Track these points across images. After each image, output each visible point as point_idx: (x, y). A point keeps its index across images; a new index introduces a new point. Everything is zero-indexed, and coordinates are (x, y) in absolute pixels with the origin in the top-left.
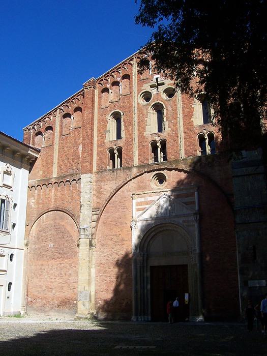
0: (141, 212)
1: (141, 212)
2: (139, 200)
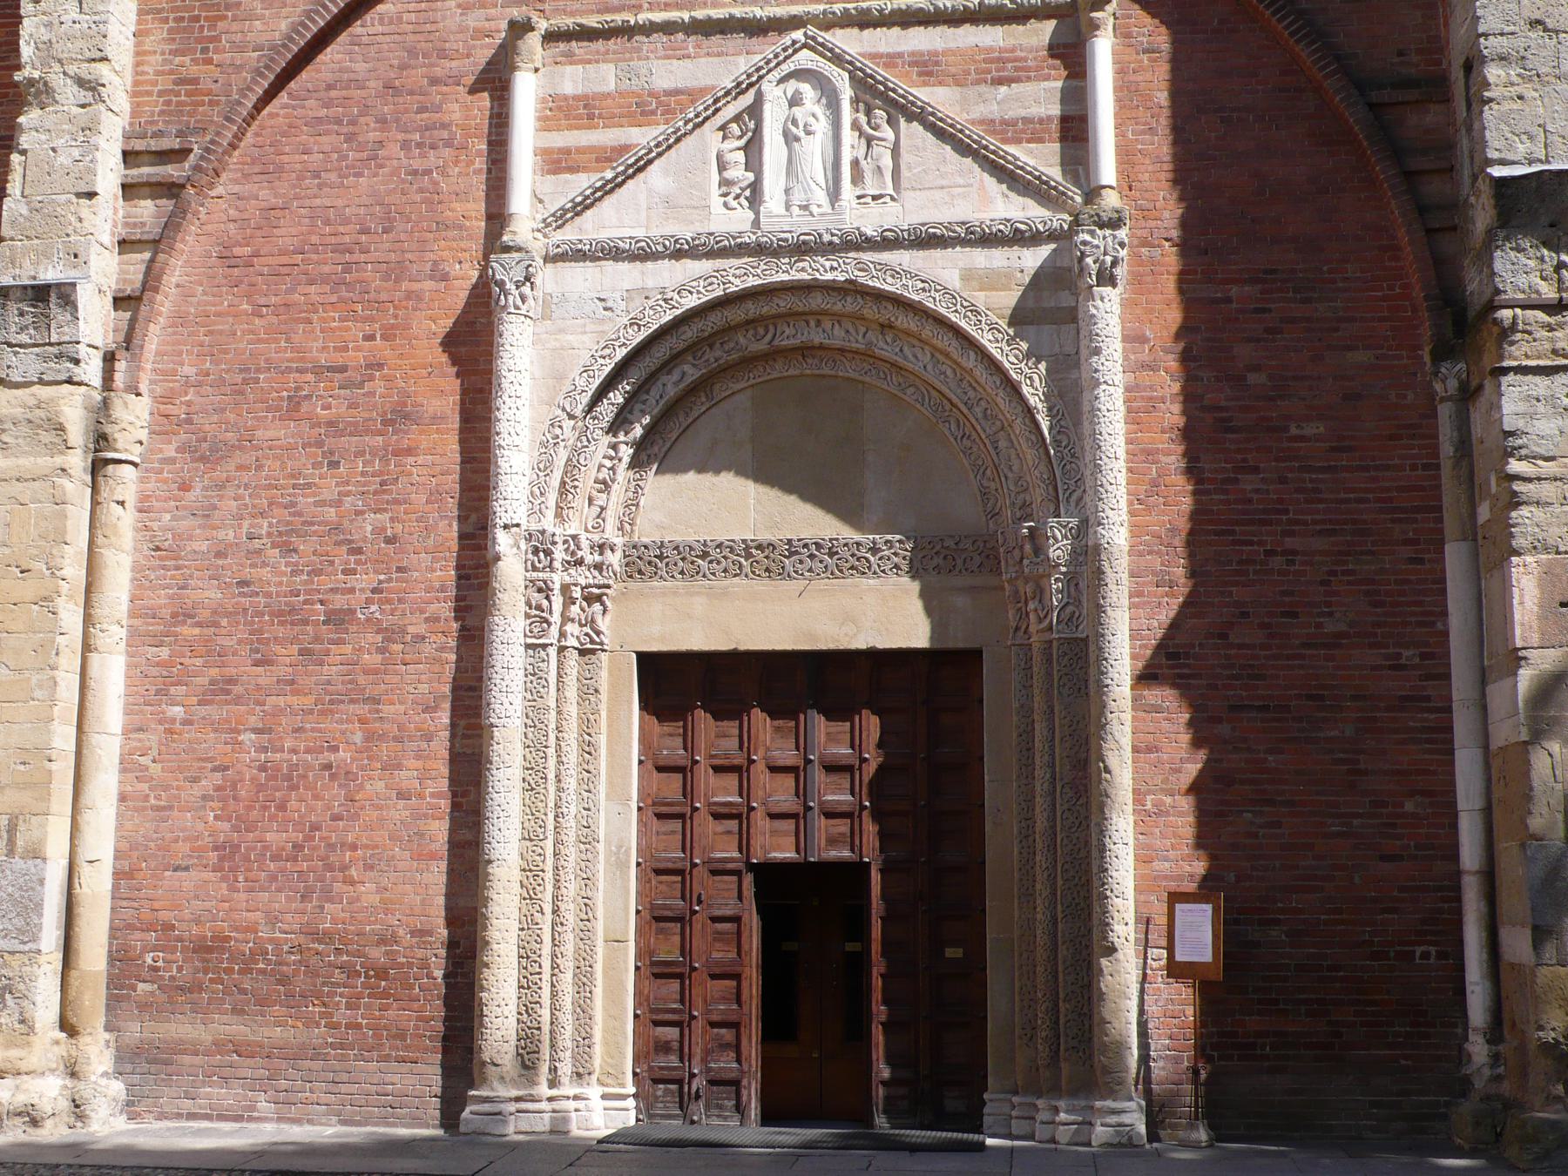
0: (582, 182)
1: (582, 182)
2: (573, 80)
